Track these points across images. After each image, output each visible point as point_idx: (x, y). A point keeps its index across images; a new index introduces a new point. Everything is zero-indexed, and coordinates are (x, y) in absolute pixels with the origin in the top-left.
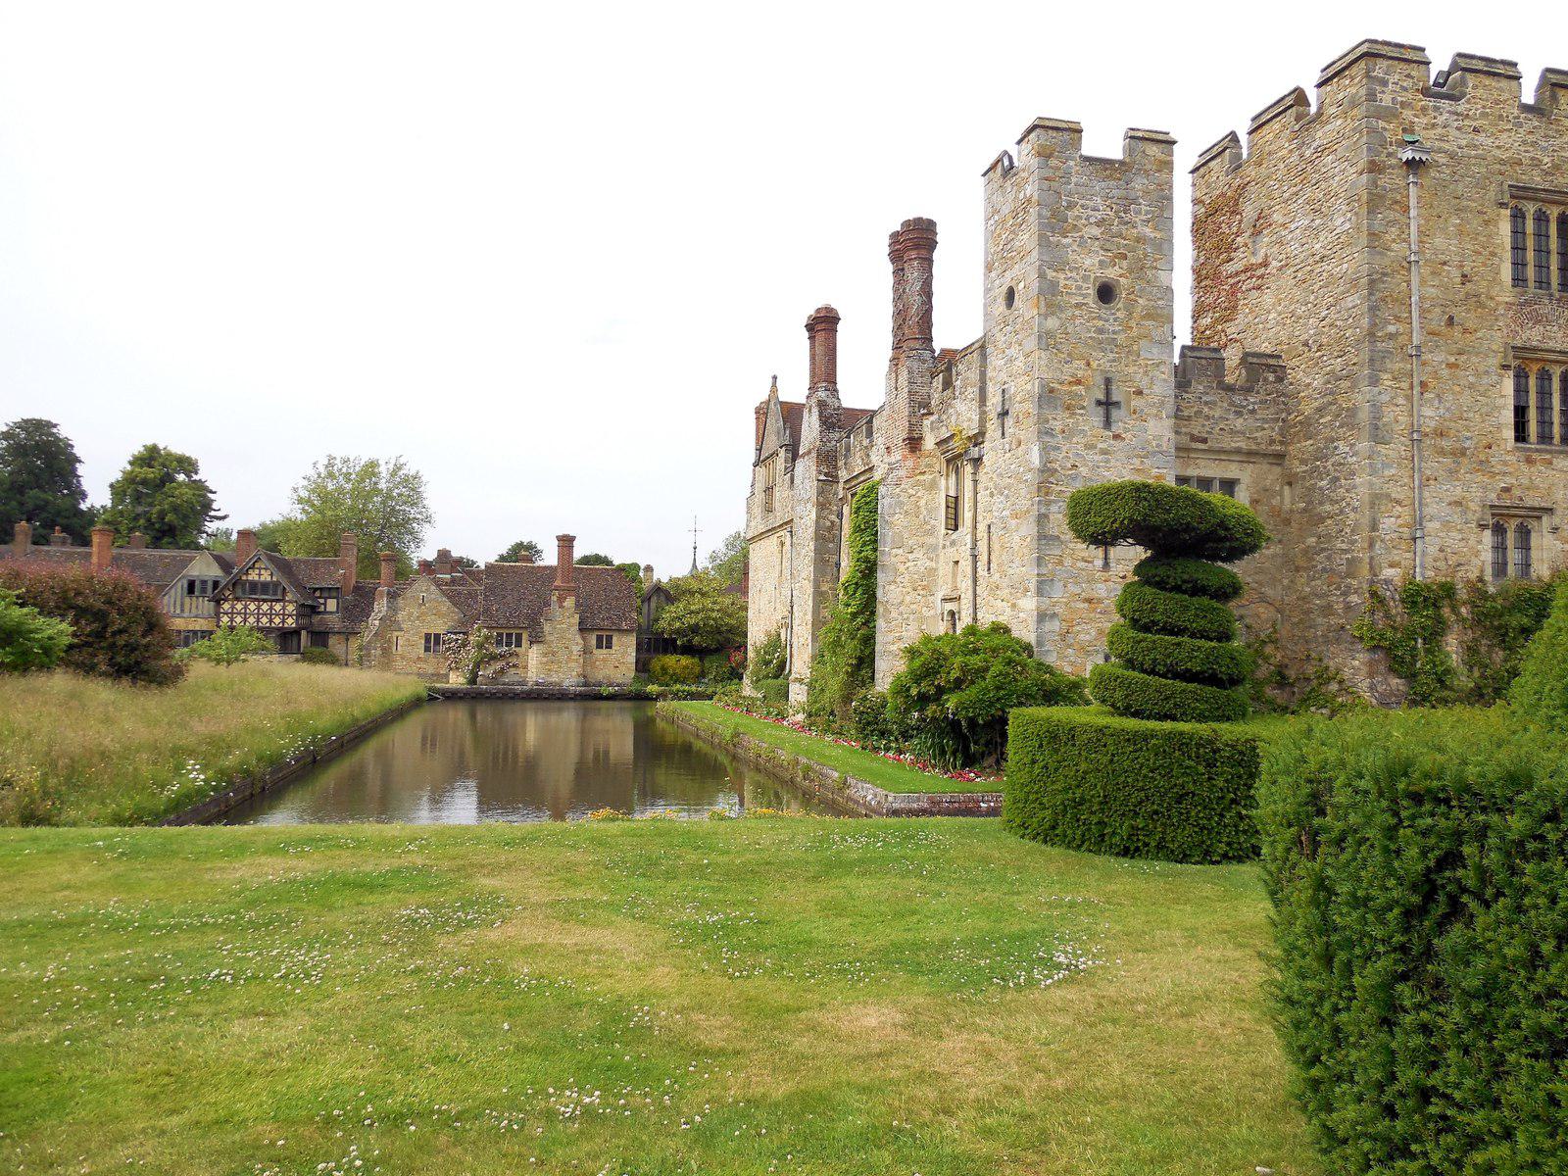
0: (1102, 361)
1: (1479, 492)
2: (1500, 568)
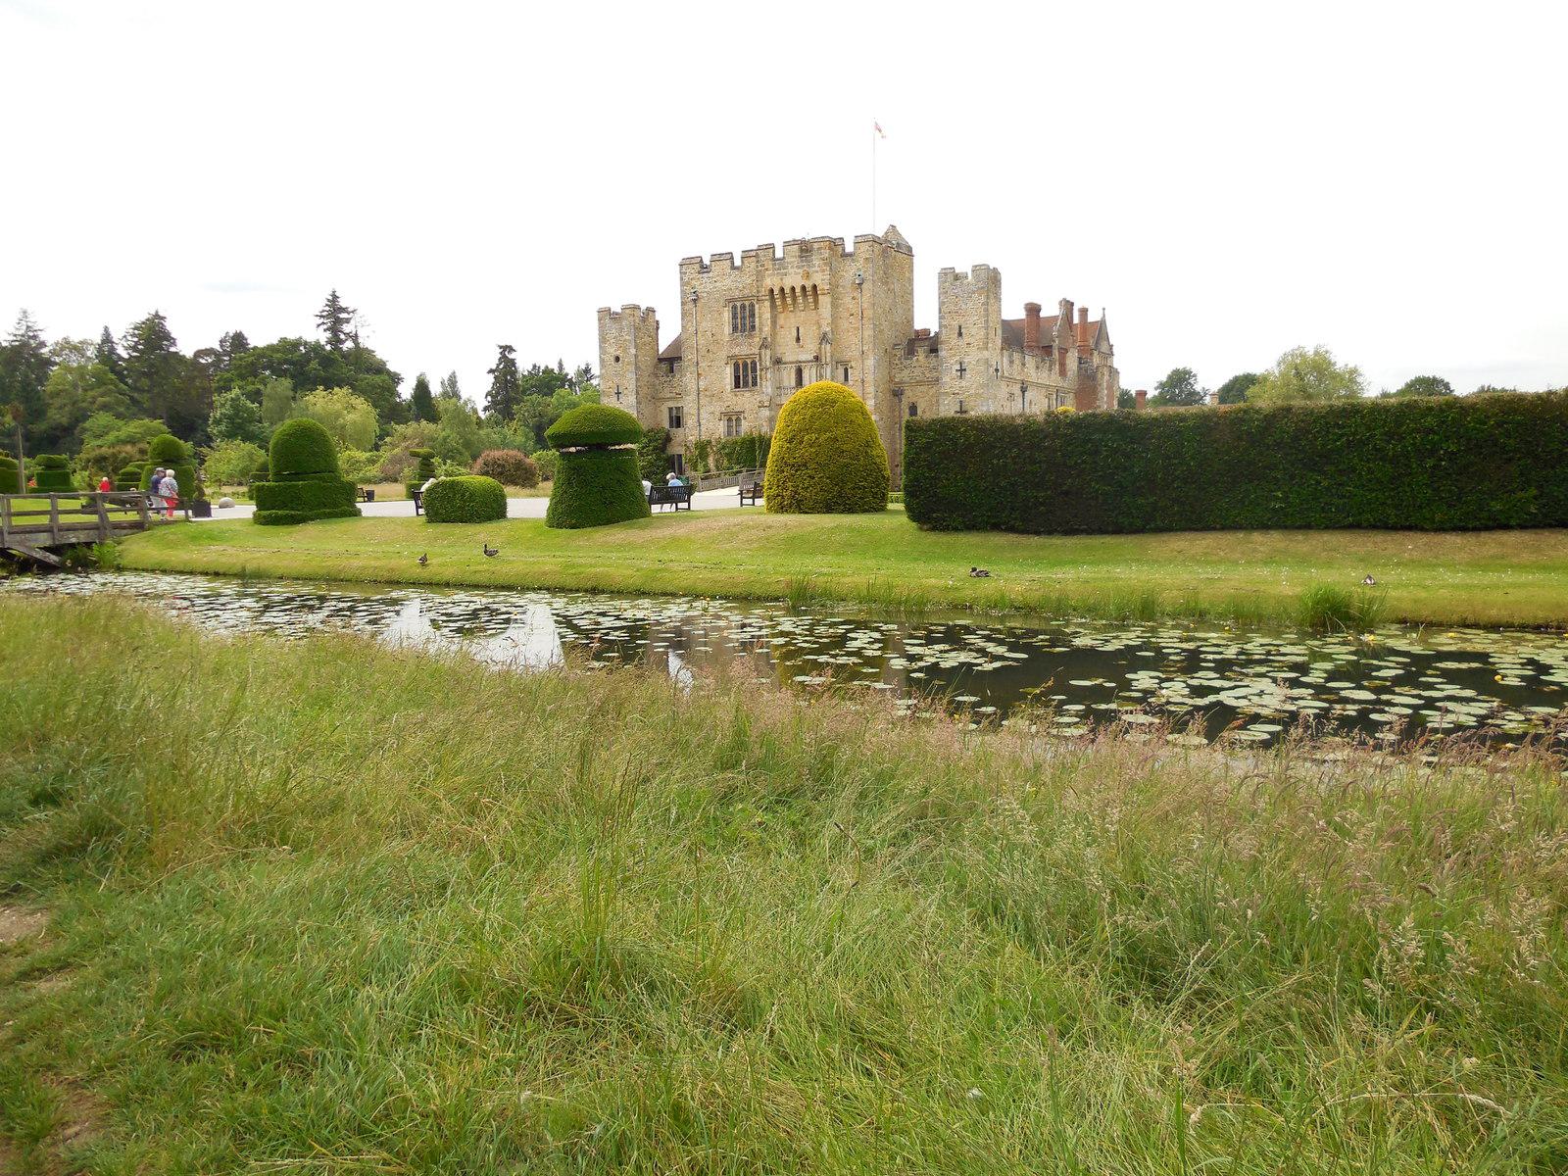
0: (616, 380)
1: (718, 408)
2: (729, 433)
